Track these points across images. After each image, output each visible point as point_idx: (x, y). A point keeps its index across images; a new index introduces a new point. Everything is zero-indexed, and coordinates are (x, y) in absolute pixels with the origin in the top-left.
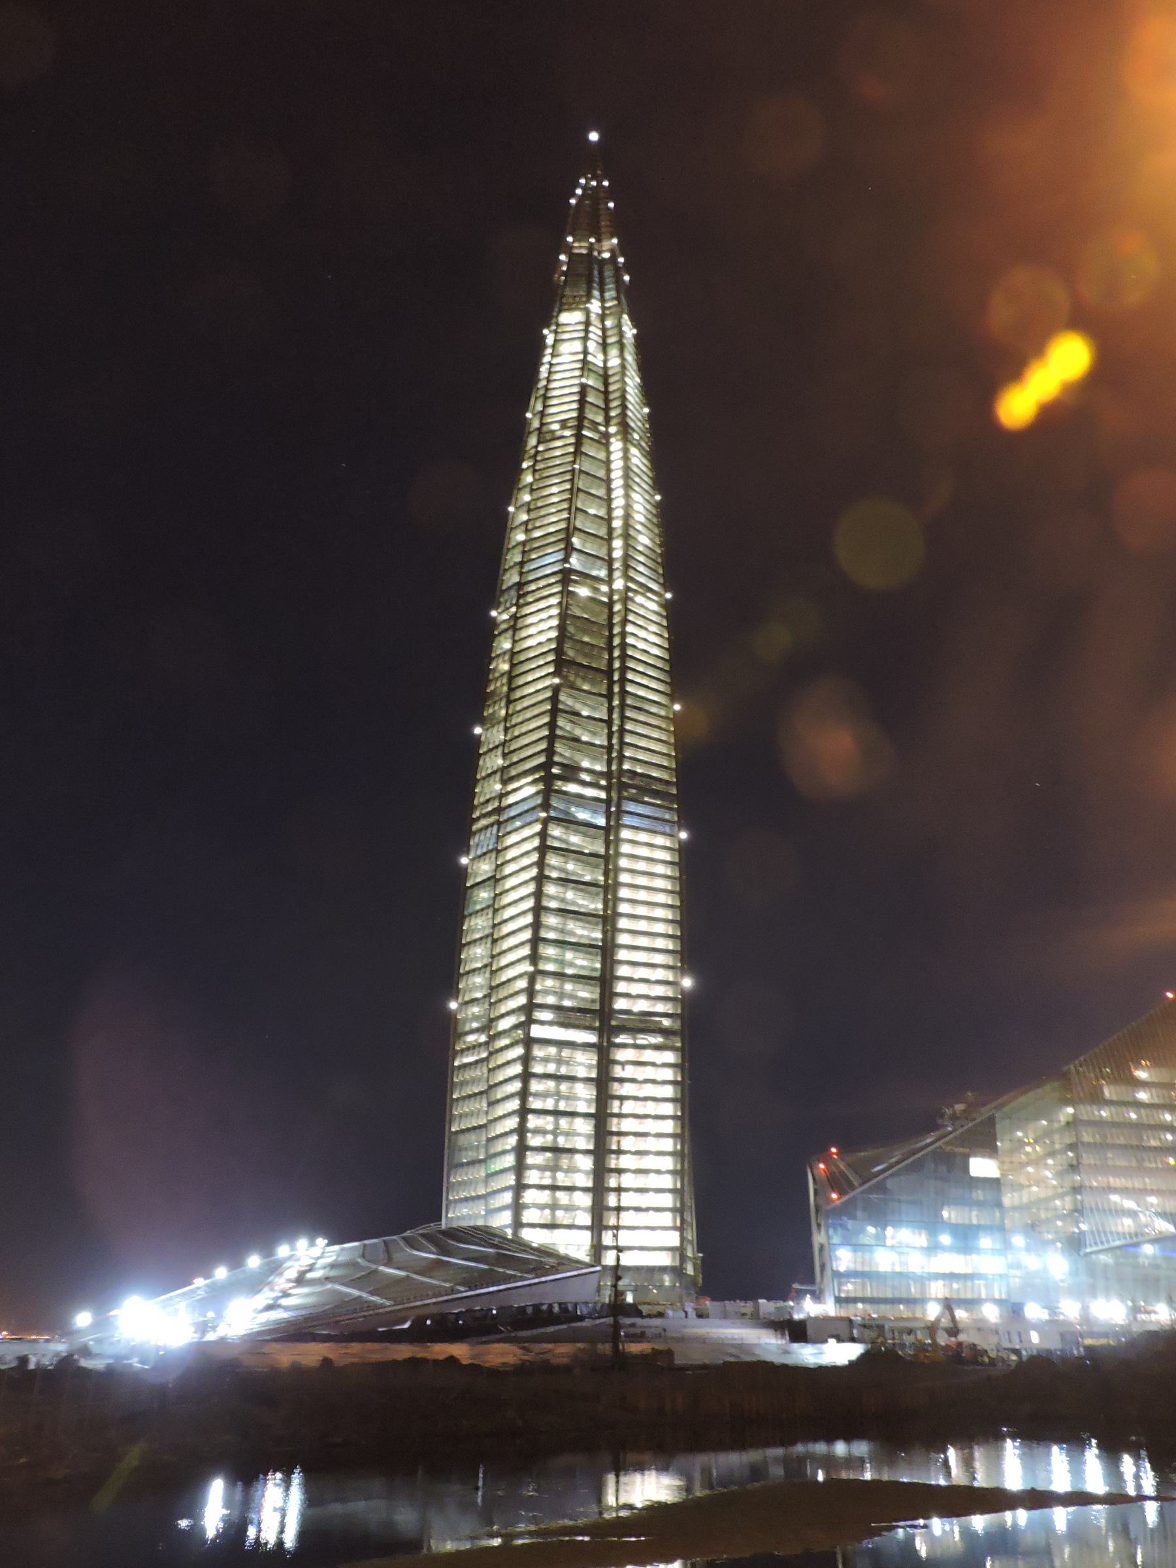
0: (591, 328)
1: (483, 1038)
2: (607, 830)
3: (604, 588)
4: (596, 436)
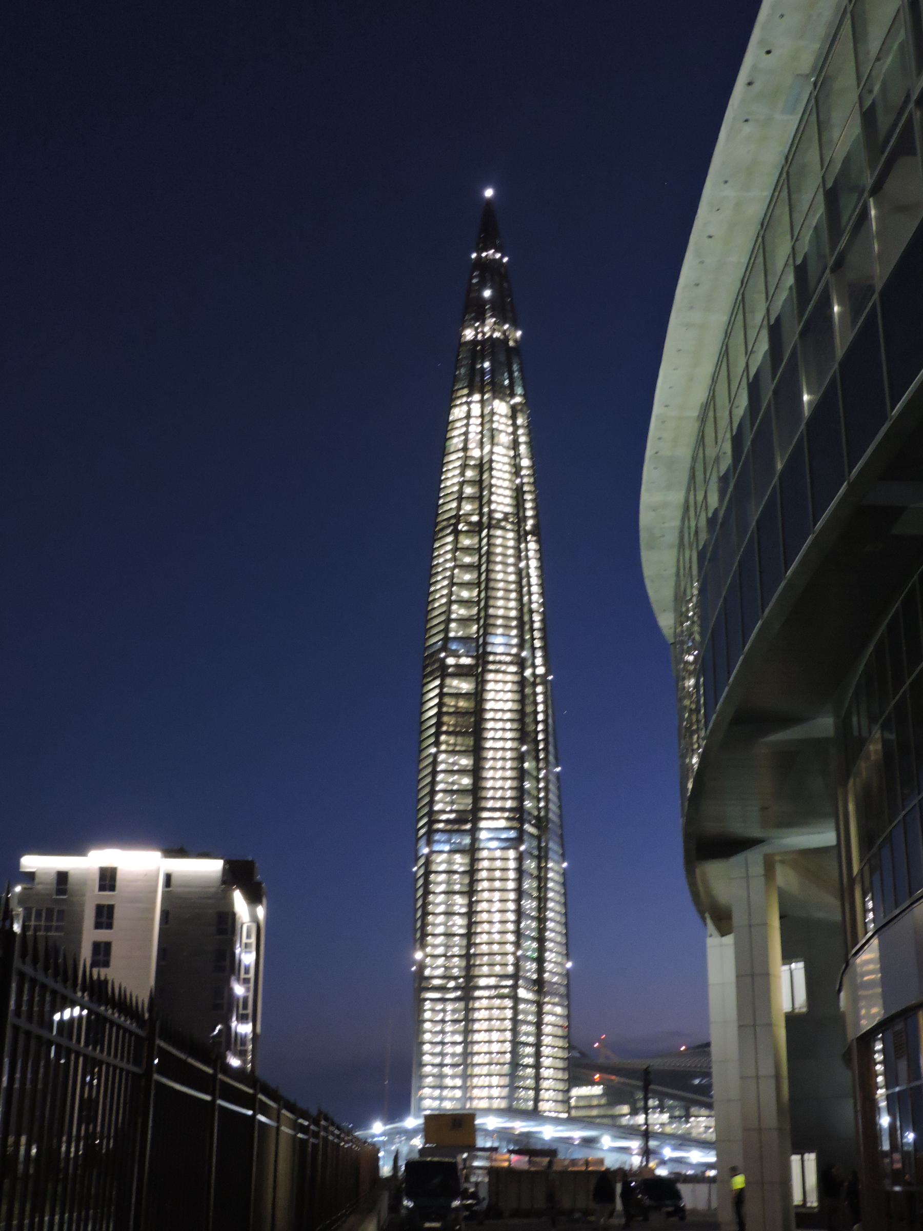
1: (452, 984)
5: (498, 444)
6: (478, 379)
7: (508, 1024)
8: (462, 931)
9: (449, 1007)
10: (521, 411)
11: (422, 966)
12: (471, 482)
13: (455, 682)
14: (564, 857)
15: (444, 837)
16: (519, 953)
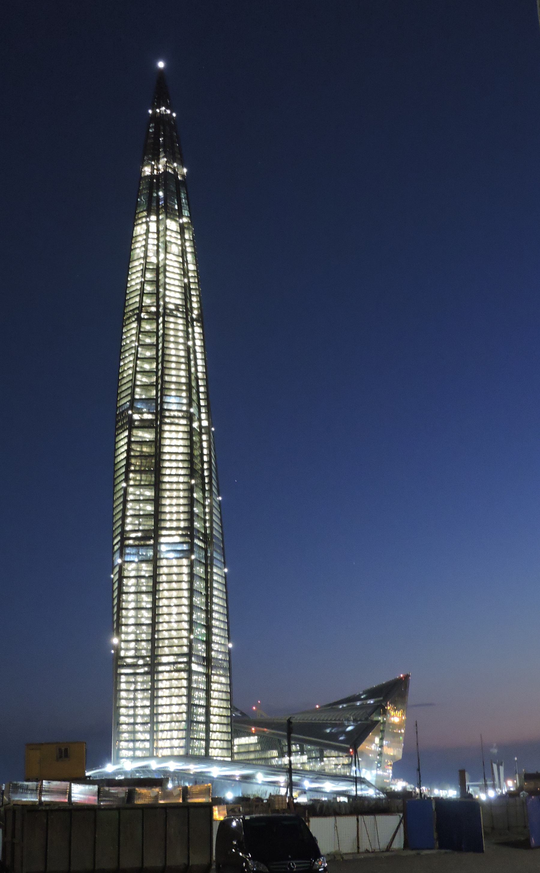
1: (141, 662)
5: (169, 253)
6: (154, 204)
7: (184, 691)
8: (149, 622)
9: (140, 679)
10: (188, 229)
11: (118, 649)
12: (150, 282)
13: (140, 433)
14: (225, 564)
15: (133, 551)
16: (192, 637)
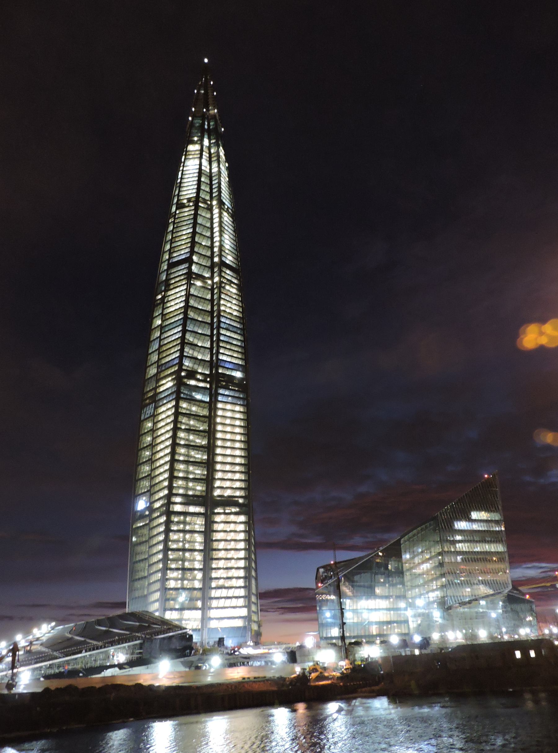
0: (204, 153)
2: (210, 403)
3: (210, 282)
4: (206, 206)
